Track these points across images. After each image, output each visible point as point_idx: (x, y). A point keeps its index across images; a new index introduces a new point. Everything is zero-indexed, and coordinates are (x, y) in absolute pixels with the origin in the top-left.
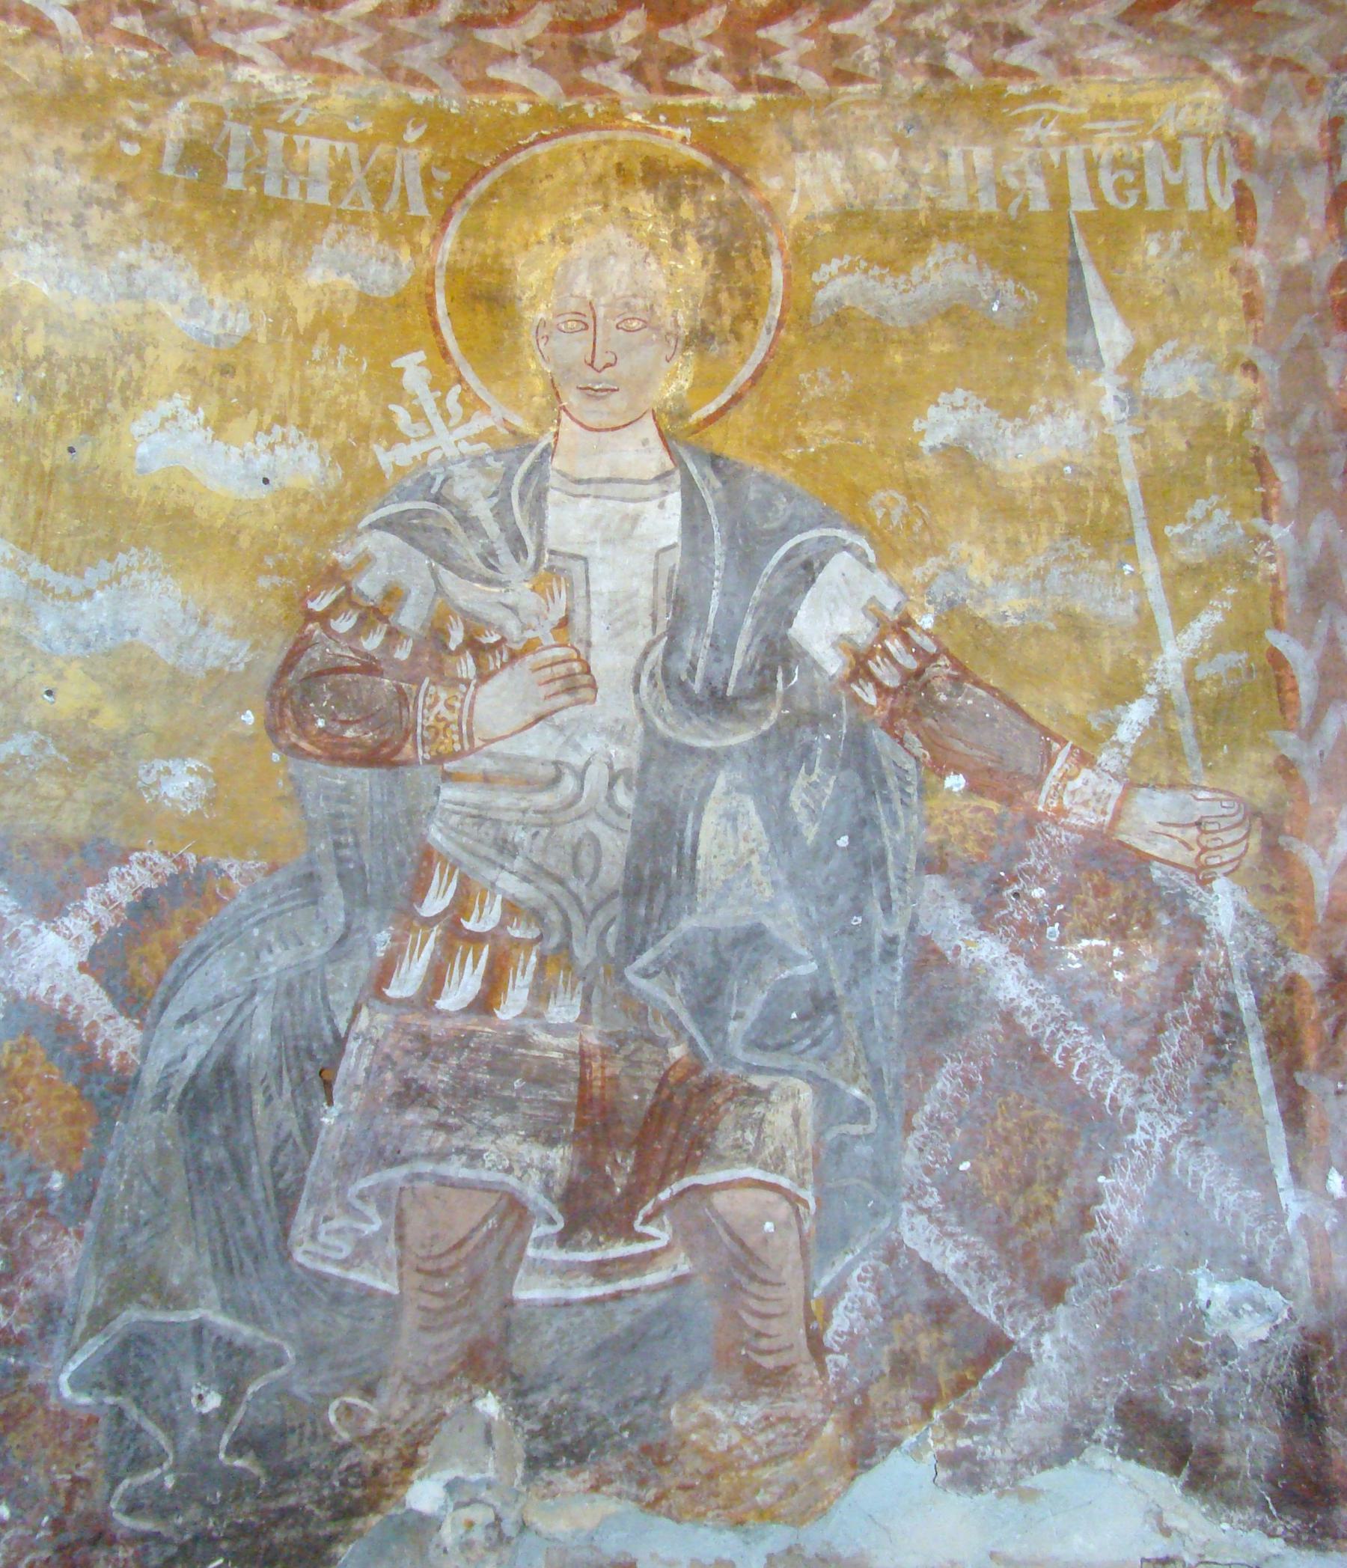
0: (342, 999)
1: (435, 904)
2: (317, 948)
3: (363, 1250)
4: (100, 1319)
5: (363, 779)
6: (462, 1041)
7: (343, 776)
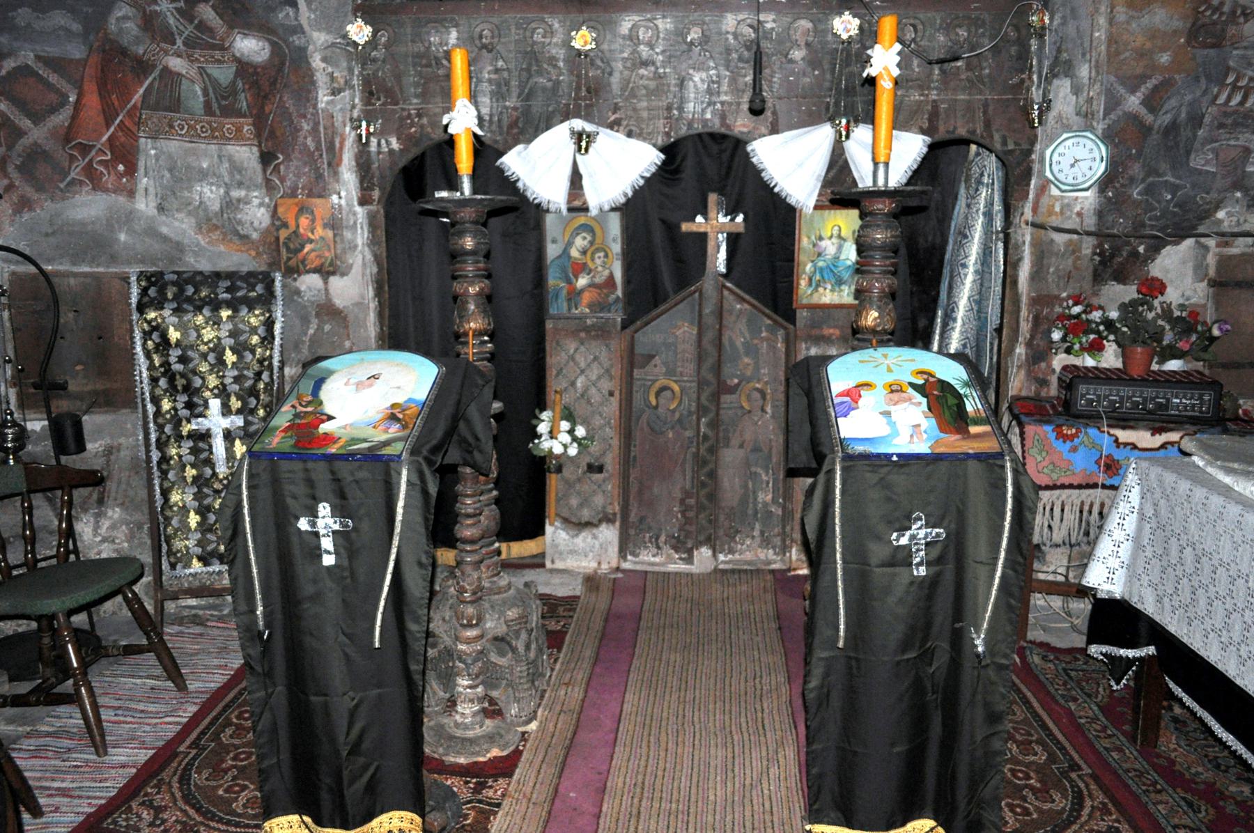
0: (1204, 105)
1: (1230, 80)
2: (1198, 93)
3: (1207, 162)
4: (1143, 180)
5: (1212, 52)
6: (1235, 112)
7: (1206, 52)
